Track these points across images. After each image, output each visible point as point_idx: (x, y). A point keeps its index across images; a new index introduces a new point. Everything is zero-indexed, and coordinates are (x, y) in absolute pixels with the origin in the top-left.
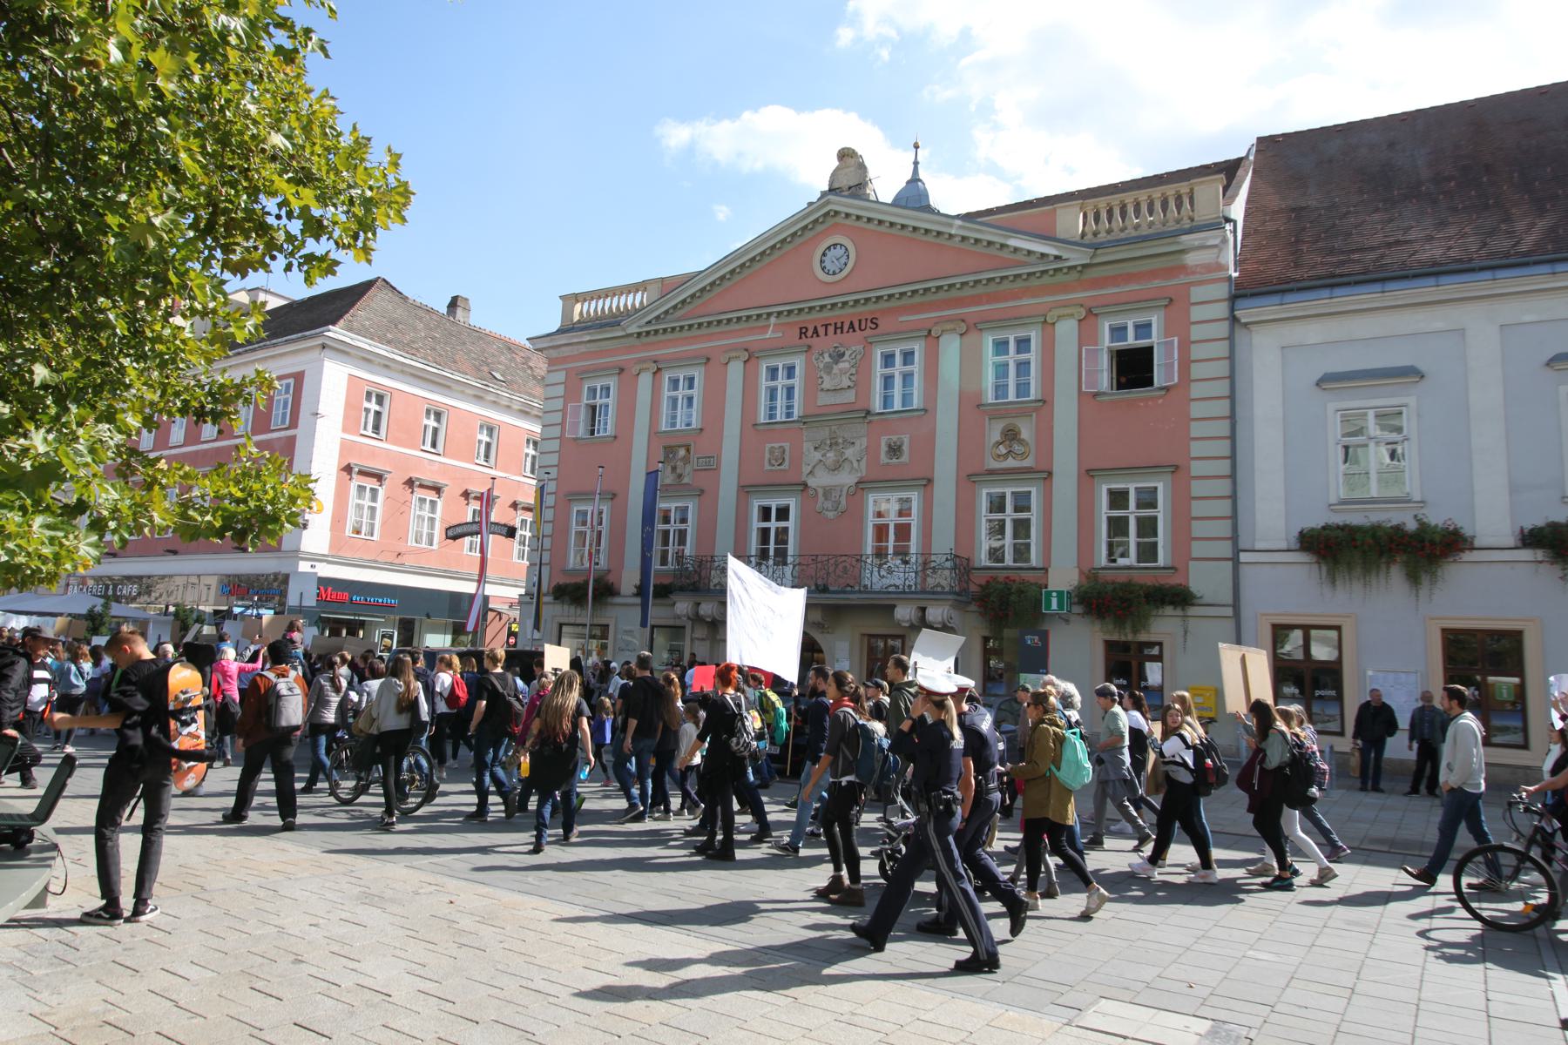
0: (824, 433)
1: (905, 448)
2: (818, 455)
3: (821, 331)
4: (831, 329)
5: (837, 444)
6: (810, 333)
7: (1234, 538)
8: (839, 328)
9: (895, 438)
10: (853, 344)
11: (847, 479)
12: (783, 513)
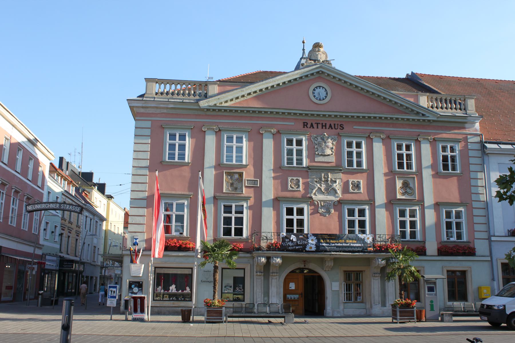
3: (315, 126)
6: (309, 126)
7: (488, 231)
12: (300, 212)
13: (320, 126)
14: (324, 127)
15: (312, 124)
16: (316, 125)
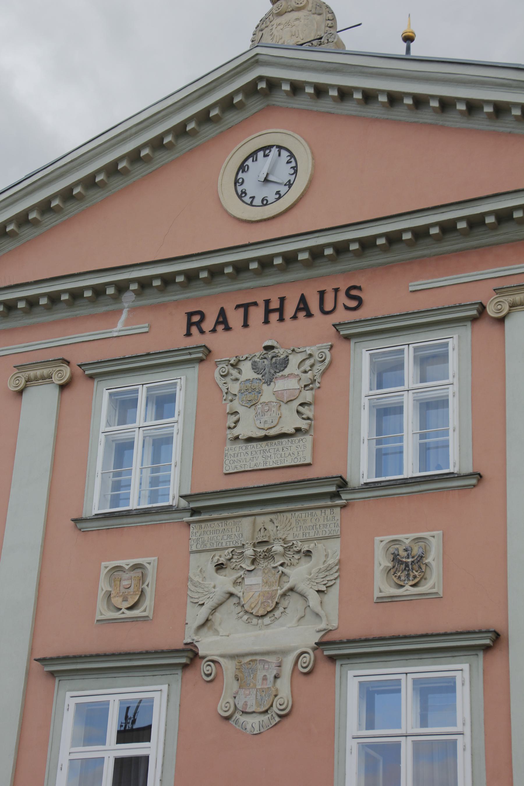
0: (241, 531)
1: (433, 558)
2: (224, 582)
3: (235, 318)
4: (257, 315)
5: (269, 556)
8: (274, 311)
9: (407, 538)
10: (308, 337)
11: (294, 634)
13: (257, 315)
14: (274, 317)
15: (222, 312)
16: (241, 310)
